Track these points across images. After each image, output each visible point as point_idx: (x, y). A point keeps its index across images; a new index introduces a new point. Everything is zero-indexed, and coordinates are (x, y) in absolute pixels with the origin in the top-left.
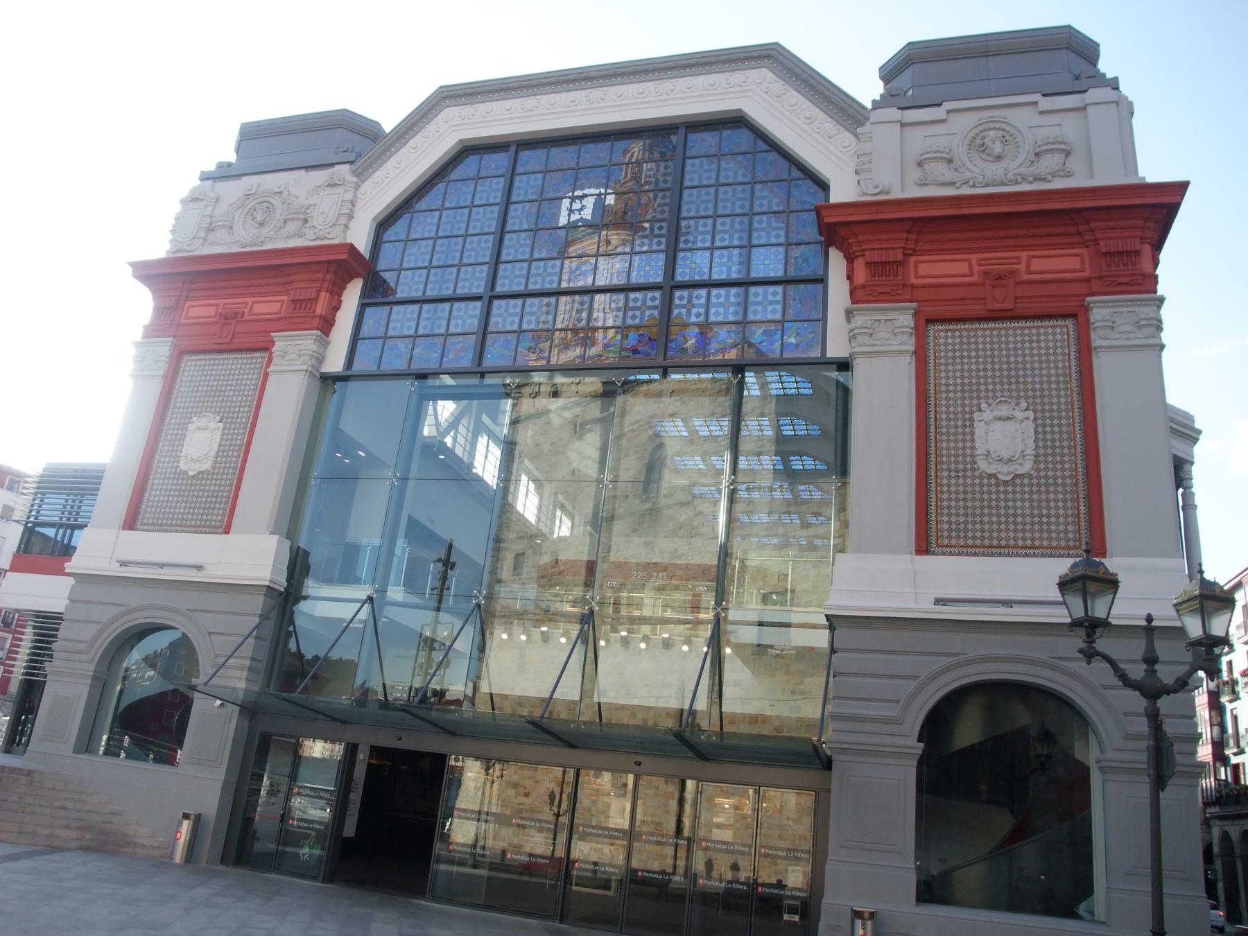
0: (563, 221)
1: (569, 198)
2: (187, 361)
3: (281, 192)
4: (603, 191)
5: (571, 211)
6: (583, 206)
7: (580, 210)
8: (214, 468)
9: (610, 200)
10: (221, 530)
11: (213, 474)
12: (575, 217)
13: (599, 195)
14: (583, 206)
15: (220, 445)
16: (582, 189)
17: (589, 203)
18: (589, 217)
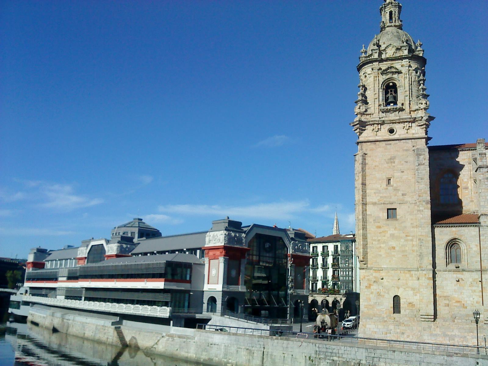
9: (270, 245)
17: (268, 245)
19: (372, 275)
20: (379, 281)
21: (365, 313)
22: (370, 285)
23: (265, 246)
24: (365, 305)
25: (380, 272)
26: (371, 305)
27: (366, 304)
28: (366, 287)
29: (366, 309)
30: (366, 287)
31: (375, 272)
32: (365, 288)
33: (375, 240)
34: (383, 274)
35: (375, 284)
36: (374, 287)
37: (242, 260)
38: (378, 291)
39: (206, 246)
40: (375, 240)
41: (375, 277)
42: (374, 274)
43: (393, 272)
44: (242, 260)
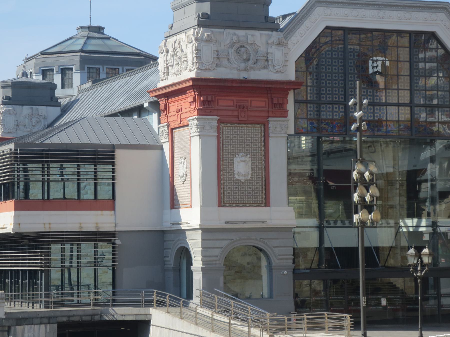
0: (371, 71)
1: (371, 60)
2: (223, 127)
3: (252, 44)
4: (384, 59)
5: (373, 67)
6: (377, 65)
7: (377, 67)
8: (252, 178)
9: (388, 63)
10: (264, 205)
11: (252, 181)
12: (375, 70)
13: (383, 60)
14: (377, 65)
15: (252, 168)
16: (376, 56)
17: (380, 63)
18: (380, 71)
23: (368, 68)
37: (273, 122)
39: (161, 84)
44: (273, 122)
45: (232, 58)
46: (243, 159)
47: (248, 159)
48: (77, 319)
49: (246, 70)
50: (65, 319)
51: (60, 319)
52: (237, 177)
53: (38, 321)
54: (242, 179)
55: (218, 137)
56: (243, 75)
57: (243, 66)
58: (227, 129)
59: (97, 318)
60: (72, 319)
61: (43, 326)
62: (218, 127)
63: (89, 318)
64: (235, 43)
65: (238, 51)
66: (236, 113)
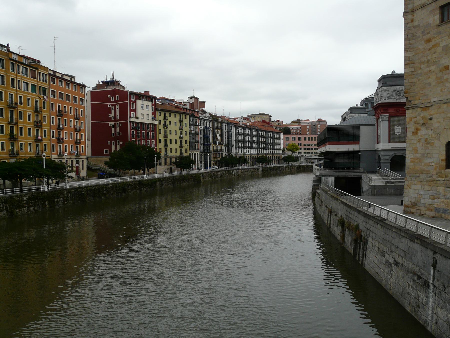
19: (419, 115)
20: (427, 123)
21: (411, 169)
22: (418, 129)
24: (412, 158)
25: (428, 110)
26: (418, 158)
27: (412, 157)
28: (413, 133)
29: (412, 164)
30: (413, 133)
31: (423, 110)
32: (411, 135)
33: (423, 63)
34: (432, 111)
35: (423, 128)
36: (422, 132)
38: (426, 137)
40: (423, 63)
41: (423, 118)
42: (422, 114)
43: (445, 106)
45: (394, 95)
46: (398, 127)
47: (400, 127)
48: (340, 176)
49: (399, 99)
50: (337, 176)
51: (335, 176)
52: (396, 133)
53: (329, 176)
54: (398, 134)
55: (389, 121)
56: (398, 101)
57: (398, 97)
58: (392, 119)
59: (346, 176)
60: (339, 176)
61: (330, 178)
62: (389, 118)
63: (345, 176)
64: (395, 91)
65: (396, 94)
66: (395, 113)
